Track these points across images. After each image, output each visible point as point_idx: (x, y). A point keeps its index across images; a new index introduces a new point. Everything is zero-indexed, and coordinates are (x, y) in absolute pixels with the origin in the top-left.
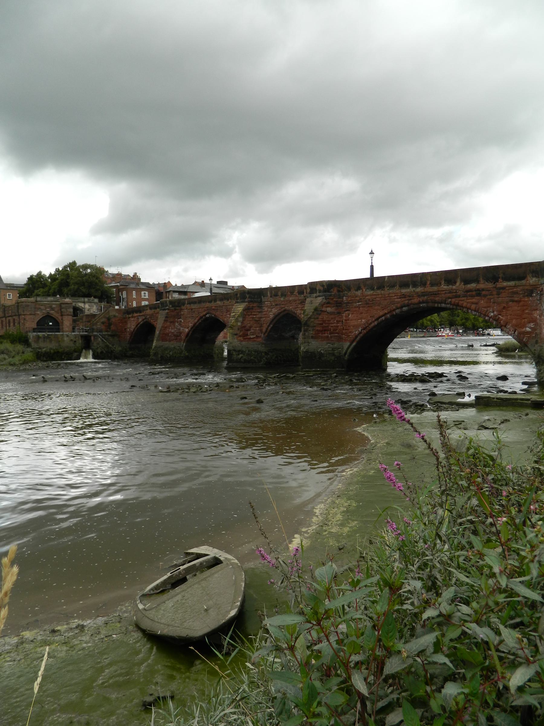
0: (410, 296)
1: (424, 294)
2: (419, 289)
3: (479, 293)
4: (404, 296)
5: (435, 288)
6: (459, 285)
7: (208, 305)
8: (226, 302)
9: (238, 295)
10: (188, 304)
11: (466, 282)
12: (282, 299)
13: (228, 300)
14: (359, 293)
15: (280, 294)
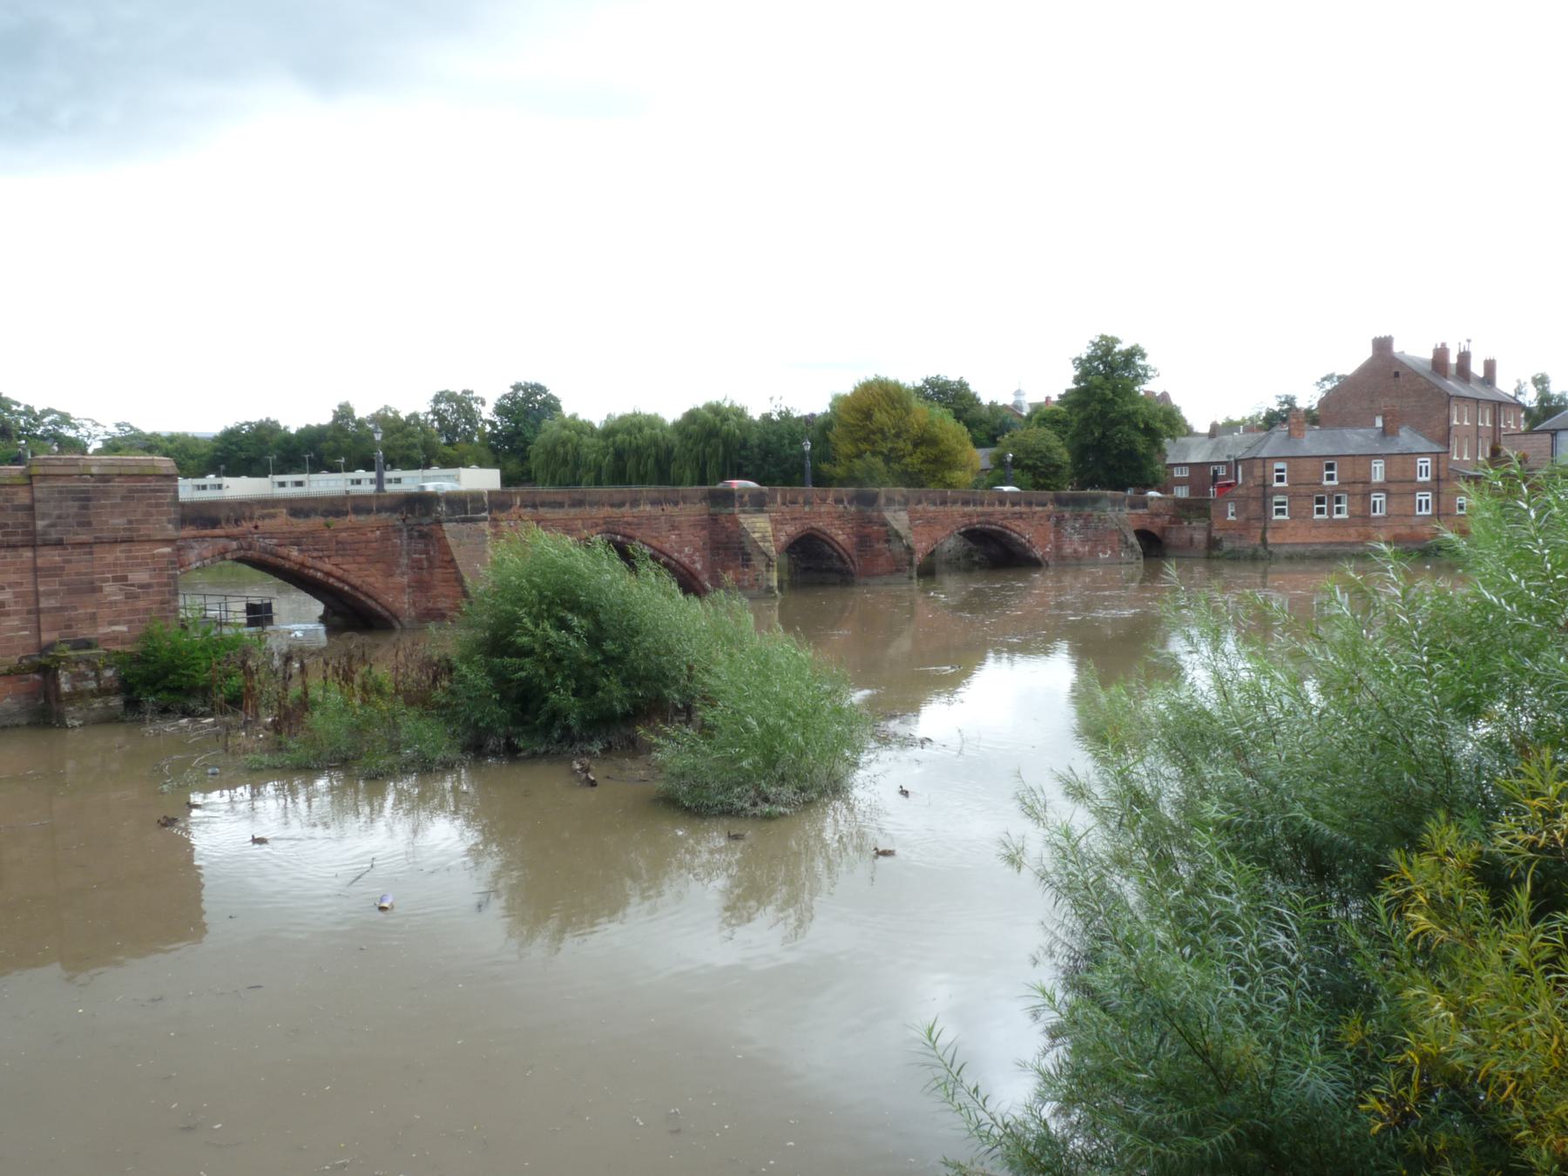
0: (970, 515)
1: (983, 514)
2: (979, 509)
3: (1020, 516)
4: (964, 515)
5: (991, 509)
6: (1008, 508)
7: (607, 511)
8: (669, 508)
9: (746, 498)
10: (524, 505)
11: (1014, 504)
12: (807, 509)
13: (676, 504)
14: (920, 507)
15: (801, 500)
